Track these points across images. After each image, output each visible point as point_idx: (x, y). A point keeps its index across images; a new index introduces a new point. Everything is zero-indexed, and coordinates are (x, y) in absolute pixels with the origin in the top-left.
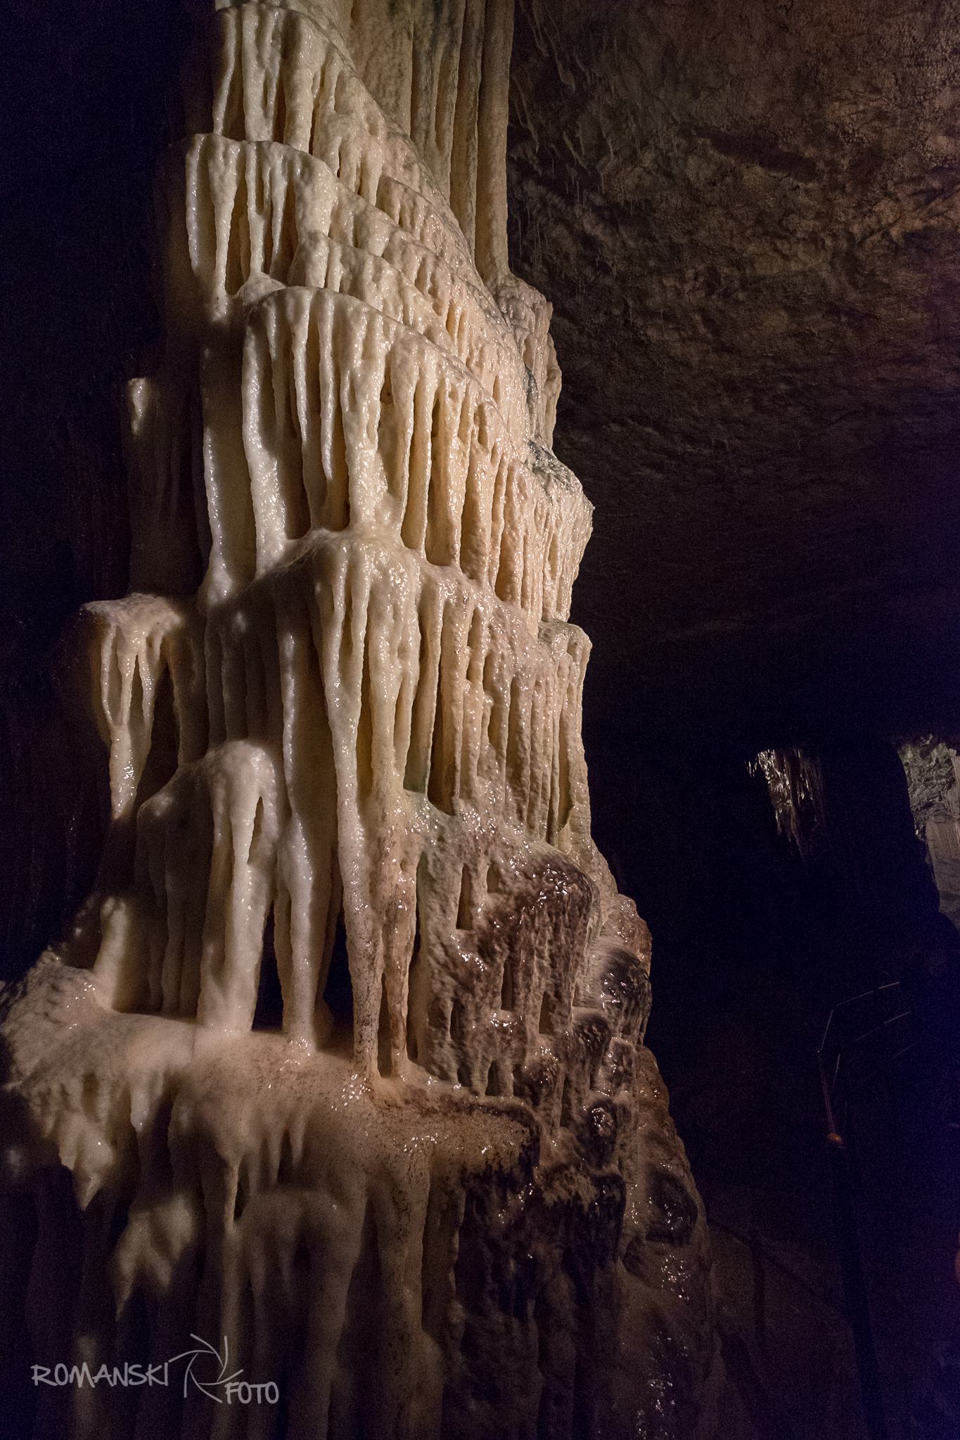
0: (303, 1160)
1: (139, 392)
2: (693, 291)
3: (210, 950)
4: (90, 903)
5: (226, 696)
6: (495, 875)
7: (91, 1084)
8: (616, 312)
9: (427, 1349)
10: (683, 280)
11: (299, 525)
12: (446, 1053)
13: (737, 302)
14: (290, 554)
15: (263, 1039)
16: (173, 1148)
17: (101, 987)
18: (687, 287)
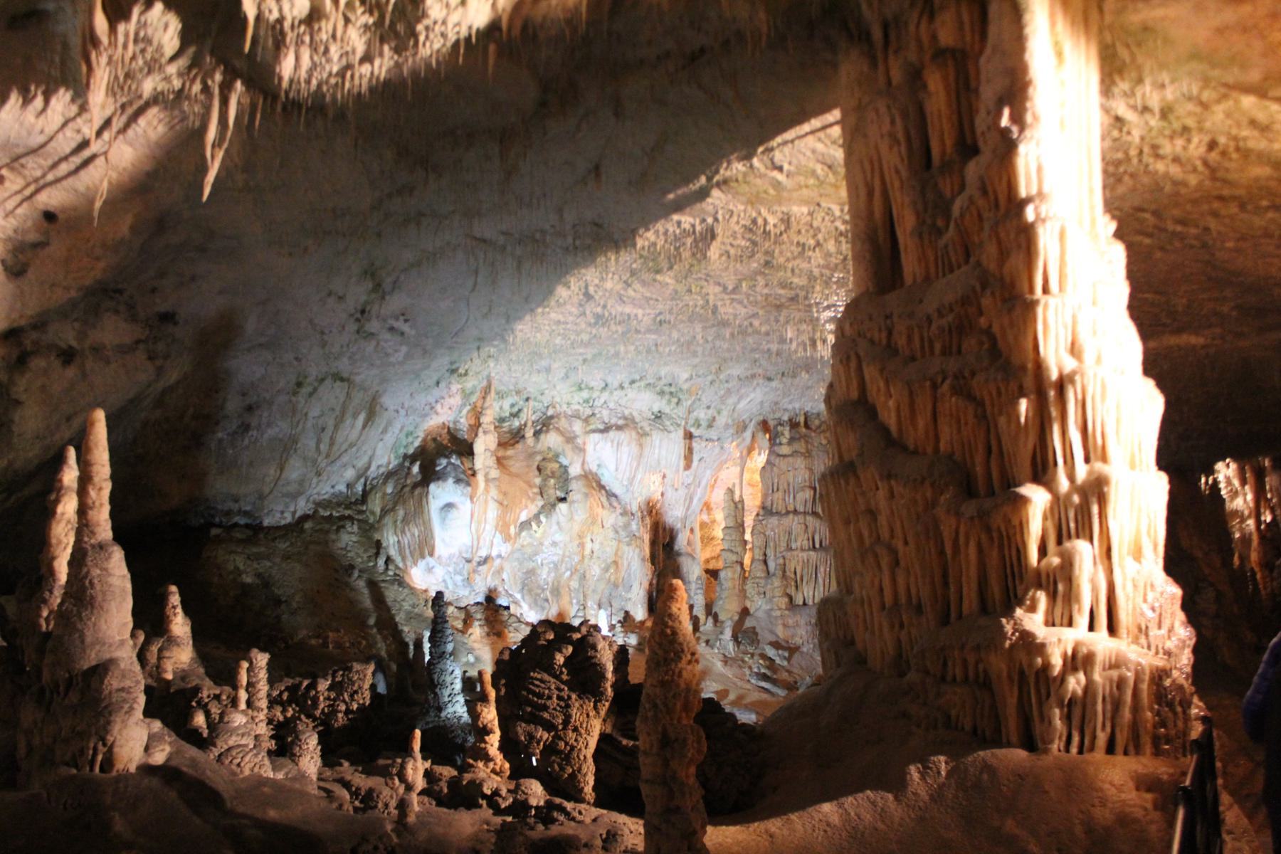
0: (1116, 664)
1: (1023, 405)
2: (1197, 147)
3: (1075, 607)
4: (1030, 594)
5: (1072, 525)
6: (1152, 586)
7: (1060, 640)
8: (1133, 152)
9: (1149, 714)
10: (1189, 141)
11: (1087, 460)
12: (1143, 640)
13: (1230, 159)
14: (1090, 473)
15: (1091, 634)
16: (1079, 660)
17: (1039, 616)
18: (1192, 146)
